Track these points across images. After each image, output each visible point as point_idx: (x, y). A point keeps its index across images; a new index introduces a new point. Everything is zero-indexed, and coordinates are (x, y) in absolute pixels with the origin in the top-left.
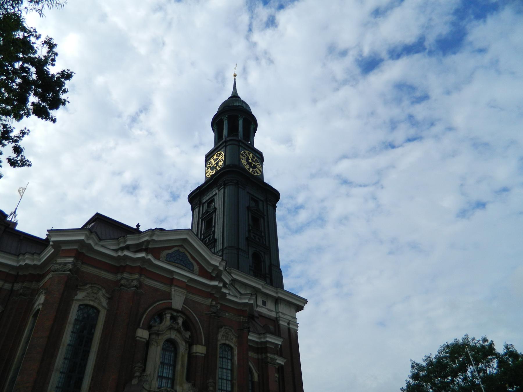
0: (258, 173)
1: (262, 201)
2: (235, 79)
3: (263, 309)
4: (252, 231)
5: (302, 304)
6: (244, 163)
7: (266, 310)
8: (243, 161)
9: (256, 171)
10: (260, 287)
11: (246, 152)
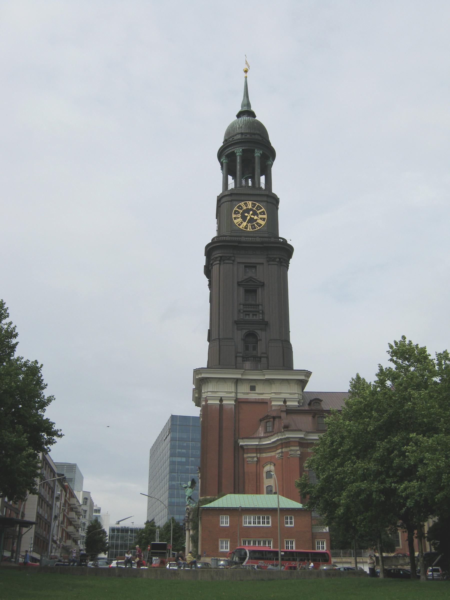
0: (261, 225)
1: (263, 264)
2: (246, 77)
3: (250, 395)
4: (242, 311)
5: (302, 377)
6: (237, 223)
7: (256, 395)
8: (235, 221)
9: (257, 224)
10: (239, 376)
11: (242, 204)
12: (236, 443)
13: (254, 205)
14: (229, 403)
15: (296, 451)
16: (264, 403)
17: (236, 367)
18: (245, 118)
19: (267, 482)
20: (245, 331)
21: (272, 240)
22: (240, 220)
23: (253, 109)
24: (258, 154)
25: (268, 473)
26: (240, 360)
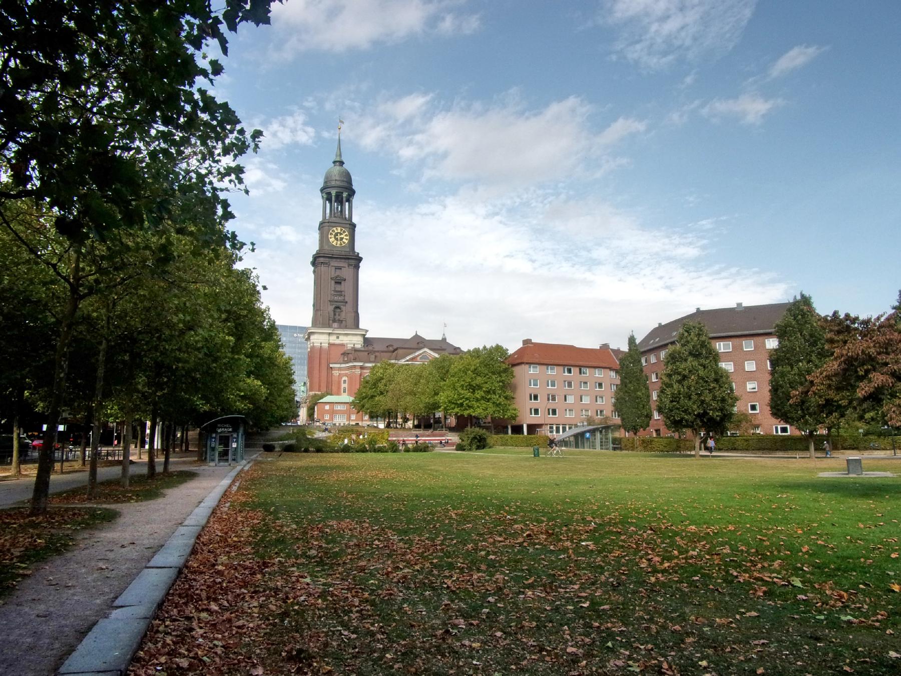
8: (331, 240)
11: (335, 229)
12: (328, 365)
13: (341, 230)
14: (326, 345)
15: (358, 371)
16: (343, 345)
17: (329, 326)
18: (338, 168)
19: (343, 386)
20: (334, 306)
21: (351, 254)
22: (333, 239)
23: (344, 159)
24: (345, 195)
25: (345, 381)
26: (331, 322)
